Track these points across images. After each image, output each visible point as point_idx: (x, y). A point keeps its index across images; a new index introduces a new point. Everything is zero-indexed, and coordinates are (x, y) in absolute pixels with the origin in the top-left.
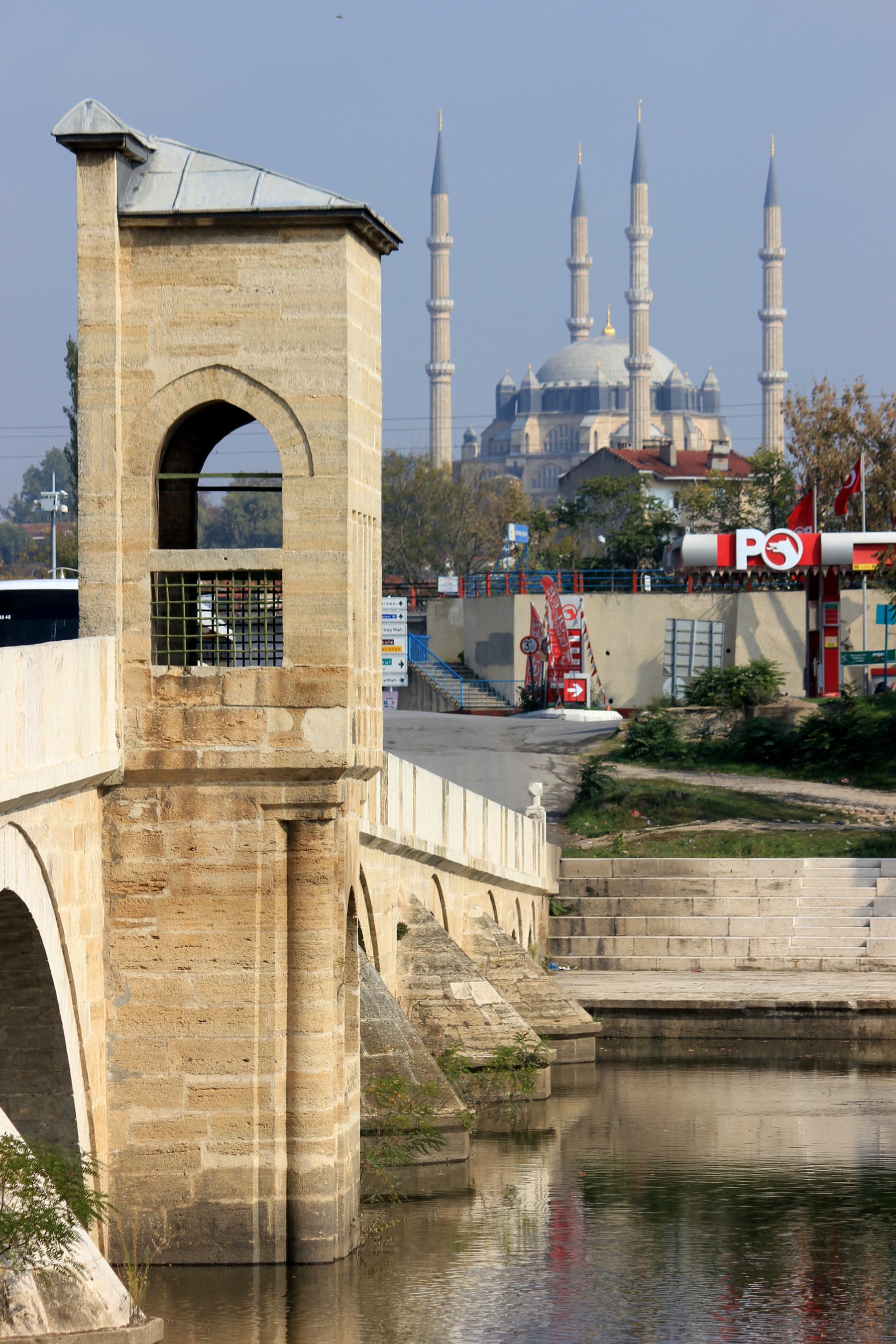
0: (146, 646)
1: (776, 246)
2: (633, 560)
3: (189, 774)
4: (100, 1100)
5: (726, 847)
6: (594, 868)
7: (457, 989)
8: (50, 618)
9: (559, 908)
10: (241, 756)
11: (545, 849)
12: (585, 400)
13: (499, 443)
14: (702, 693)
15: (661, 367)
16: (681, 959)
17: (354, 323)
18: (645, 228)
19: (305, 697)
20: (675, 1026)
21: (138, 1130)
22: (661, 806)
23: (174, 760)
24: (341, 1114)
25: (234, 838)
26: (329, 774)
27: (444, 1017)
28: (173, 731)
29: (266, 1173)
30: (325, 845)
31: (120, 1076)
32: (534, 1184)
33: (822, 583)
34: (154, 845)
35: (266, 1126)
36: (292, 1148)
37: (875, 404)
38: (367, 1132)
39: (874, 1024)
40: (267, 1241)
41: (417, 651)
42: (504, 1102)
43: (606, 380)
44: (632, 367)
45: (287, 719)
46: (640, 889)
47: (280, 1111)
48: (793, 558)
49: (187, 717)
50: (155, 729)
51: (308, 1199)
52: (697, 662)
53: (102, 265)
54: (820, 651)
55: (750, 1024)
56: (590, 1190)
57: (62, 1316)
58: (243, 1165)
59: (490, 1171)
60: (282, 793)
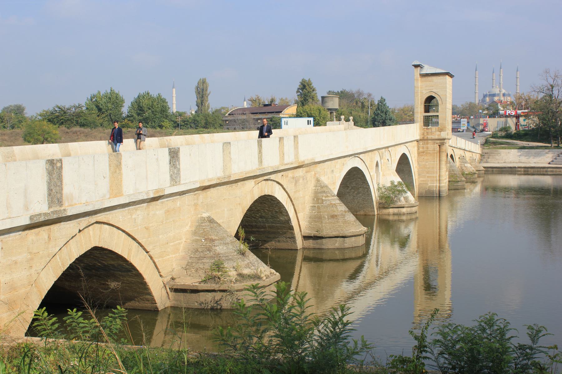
0: (422, 124)
1: (518, 76)
2: (495, 114)
3: (427, 139)
4: (417, 177)
5: (503, 148)
6: (486, 151)
7: (466, 165)
8: (412, 121)
9: (482, 155)
10: (433, 137)
11: (480, 148)
12: (494, 95)
13: (483, 101)
14: (501, 130)
15: (503, 91)
16: (497, 162)
17: (448, 86)
18: (502, 75)
19: (441, 130)
20: (495, 169)
21: (421, 181)
22: (494, 143)
23: (426, 138)
24: (445, 179)
25: (433, 147)
26: (444, 139)
27: (464, 168)
28: (425, 134)
29: (436, 186)
30: (443, 148)
31: (419, 175)
32: (478, 189)
33: (517, 117)
34: (423, 148)
35: (436, 181)
36: (439, 183)
37: (525, 95)
38: (449, 182)
39: (519, 169)
40: (436, 194)
41: (468, 125)
42: (471, 179)
43: (497, 93)
44: (500, 91)
45: (439, 133)
46: (492, 153)
47: (438, 179)
48: (514, 113)
49: (427, 133)
50: (423, 134)
51: (441, 189)
52: (501, 126)
53: (417, 80)
54: (517, 125)
55: (504, 169)
56: (485, 189)
57: (406, 202)
58: (434, 185)
59: (469, 186)
60: (438, 142)
